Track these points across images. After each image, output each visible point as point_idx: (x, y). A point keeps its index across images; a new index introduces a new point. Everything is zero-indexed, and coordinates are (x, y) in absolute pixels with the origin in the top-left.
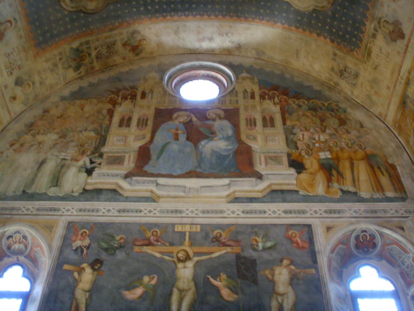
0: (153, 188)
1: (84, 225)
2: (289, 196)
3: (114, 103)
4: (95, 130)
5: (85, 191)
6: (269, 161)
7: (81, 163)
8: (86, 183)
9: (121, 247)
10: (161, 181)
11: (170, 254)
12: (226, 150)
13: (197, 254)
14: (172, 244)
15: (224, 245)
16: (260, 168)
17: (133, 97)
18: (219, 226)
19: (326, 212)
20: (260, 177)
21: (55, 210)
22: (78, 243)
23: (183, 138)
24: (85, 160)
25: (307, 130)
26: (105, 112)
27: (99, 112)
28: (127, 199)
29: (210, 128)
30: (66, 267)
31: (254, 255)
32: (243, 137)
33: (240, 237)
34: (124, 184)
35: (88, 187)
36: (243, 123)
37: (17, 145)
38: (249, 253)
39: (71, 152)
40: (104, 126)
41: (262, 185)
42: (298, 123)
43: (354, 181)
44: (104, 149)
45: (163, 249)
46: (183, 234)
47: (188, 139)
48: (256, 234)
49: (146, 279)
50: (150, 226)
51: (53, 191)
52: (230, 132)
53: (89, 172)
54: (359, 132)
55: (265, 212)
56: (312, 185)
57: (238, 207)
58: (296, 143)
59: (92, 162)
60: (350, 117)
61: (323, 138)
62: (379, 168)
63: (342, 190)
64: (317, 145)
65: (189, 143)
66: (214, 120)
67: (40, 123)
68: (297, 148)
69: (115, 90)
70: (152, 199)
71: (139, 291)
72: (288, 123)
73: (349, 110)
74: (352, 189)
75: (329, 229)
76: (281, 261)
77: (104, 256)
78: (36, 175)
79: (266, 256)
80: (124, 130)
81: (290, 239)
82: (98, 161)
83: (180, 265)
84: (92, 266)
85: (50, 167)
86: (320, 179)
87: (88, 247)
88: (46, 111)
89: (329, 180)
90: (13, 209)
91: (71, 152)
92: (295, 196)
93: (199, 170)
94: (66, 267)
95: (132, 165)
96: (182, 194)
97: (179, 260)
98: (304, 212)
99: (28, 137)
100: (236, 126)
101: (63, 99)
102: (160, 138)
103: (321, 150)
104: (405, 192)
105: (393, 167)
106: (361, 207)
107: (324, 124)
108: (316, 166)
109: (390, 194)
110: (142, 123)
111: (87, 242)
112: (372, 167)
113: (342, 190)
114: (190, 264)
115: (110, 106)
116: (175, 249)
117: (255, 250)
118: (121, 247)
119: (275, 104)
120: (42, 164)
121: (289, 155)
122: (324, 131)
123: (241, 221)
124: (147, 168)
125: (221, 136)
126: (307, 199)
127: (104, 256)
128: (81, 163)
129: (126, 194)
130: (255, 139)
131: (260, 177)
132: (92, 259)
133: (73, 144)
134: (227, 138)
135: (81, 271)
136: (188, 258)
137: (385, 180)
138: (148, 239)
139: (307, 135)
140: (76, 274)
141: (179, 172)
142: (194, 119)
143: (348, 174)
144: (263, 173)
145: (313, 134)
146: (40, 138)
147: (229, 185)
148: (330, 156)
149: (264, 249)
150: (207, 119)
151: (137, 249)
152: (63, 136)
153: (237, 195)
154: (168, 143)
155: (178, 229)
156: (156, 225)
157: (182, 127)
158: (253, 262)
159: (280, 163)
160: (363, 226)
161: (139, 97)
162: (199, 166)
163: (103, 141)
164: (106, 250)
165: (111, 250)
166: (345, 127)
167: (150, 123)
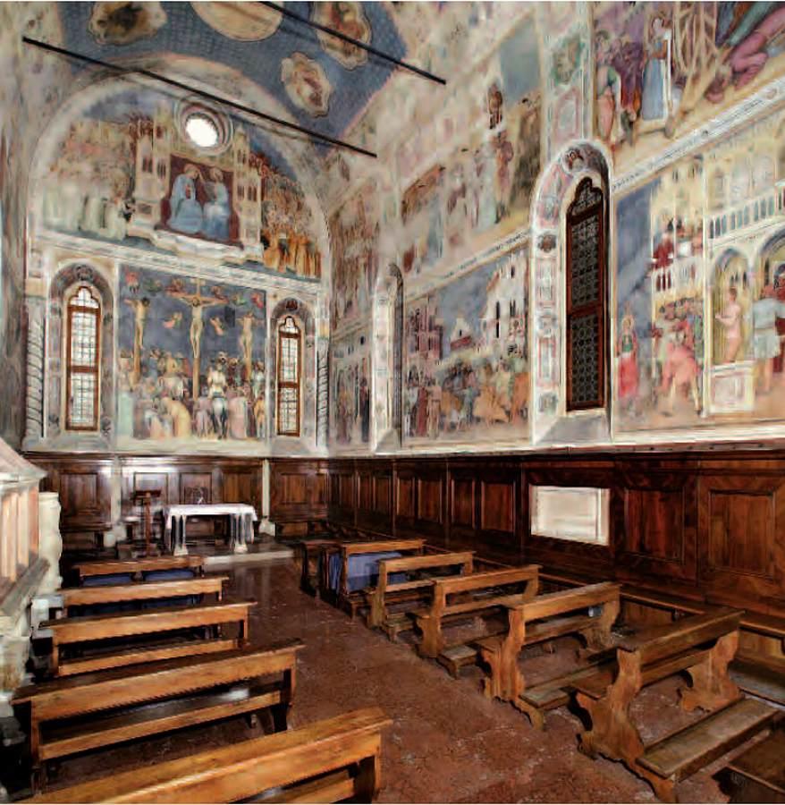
0: (172, 242)
4: (124, 169)
5: (127, 237)
9: (159, 290)
10: (180, 237)
12: (223, 217)
15: (218, 297)
16: (243, 239)
20: (242, 247)
21: (110, 252)
24: (121, 204)
27: (123, 144)
32: (234, 205)
33: (228, 295)
34: (155, 236)
35: (130, 234)
38: (233, 306)
40: (131, 166)
47: (197, 198)
49: (176, 316)
50: (176, 277)
53: (127, 217)
57: (227, 271)
58: (266, 221)
59: (128, 208)
61: (285, 219)
66: (215, 181)
69: (133, 117)
70: (173, 252)
72: (265, 199)
74: (293, 269)
76: (248, 313)
77: (149, 296)
83: (194, 308)
85: (95, 203)
86: (277, 255)
88: (73, 129)
89: (282, 258)
100: (230, 193)
103: (283, 231)
107: (289, 206)
110: (162, 171)
111: (136, 284)
116: (191, 297)
118: (159, 290)
119: (259, 174)
120: (86, 201)
121: (262, 232)
122: (286, 213)
131: (242, 247)
134: (224, 205)
135: (136, 304)
136: (198, 304)
137: (312, 265)
138: (175, 287)
140: (133, 307)
146: (76, 166)
147: (222, 251)
150: (211, 180)
152: (97, 170)
153: (230, 260)
154: (182, 200)
158: (234, 312)
159: (255, 236)
164: (150, 291)
165: (153, 292)
167: (168, 170)
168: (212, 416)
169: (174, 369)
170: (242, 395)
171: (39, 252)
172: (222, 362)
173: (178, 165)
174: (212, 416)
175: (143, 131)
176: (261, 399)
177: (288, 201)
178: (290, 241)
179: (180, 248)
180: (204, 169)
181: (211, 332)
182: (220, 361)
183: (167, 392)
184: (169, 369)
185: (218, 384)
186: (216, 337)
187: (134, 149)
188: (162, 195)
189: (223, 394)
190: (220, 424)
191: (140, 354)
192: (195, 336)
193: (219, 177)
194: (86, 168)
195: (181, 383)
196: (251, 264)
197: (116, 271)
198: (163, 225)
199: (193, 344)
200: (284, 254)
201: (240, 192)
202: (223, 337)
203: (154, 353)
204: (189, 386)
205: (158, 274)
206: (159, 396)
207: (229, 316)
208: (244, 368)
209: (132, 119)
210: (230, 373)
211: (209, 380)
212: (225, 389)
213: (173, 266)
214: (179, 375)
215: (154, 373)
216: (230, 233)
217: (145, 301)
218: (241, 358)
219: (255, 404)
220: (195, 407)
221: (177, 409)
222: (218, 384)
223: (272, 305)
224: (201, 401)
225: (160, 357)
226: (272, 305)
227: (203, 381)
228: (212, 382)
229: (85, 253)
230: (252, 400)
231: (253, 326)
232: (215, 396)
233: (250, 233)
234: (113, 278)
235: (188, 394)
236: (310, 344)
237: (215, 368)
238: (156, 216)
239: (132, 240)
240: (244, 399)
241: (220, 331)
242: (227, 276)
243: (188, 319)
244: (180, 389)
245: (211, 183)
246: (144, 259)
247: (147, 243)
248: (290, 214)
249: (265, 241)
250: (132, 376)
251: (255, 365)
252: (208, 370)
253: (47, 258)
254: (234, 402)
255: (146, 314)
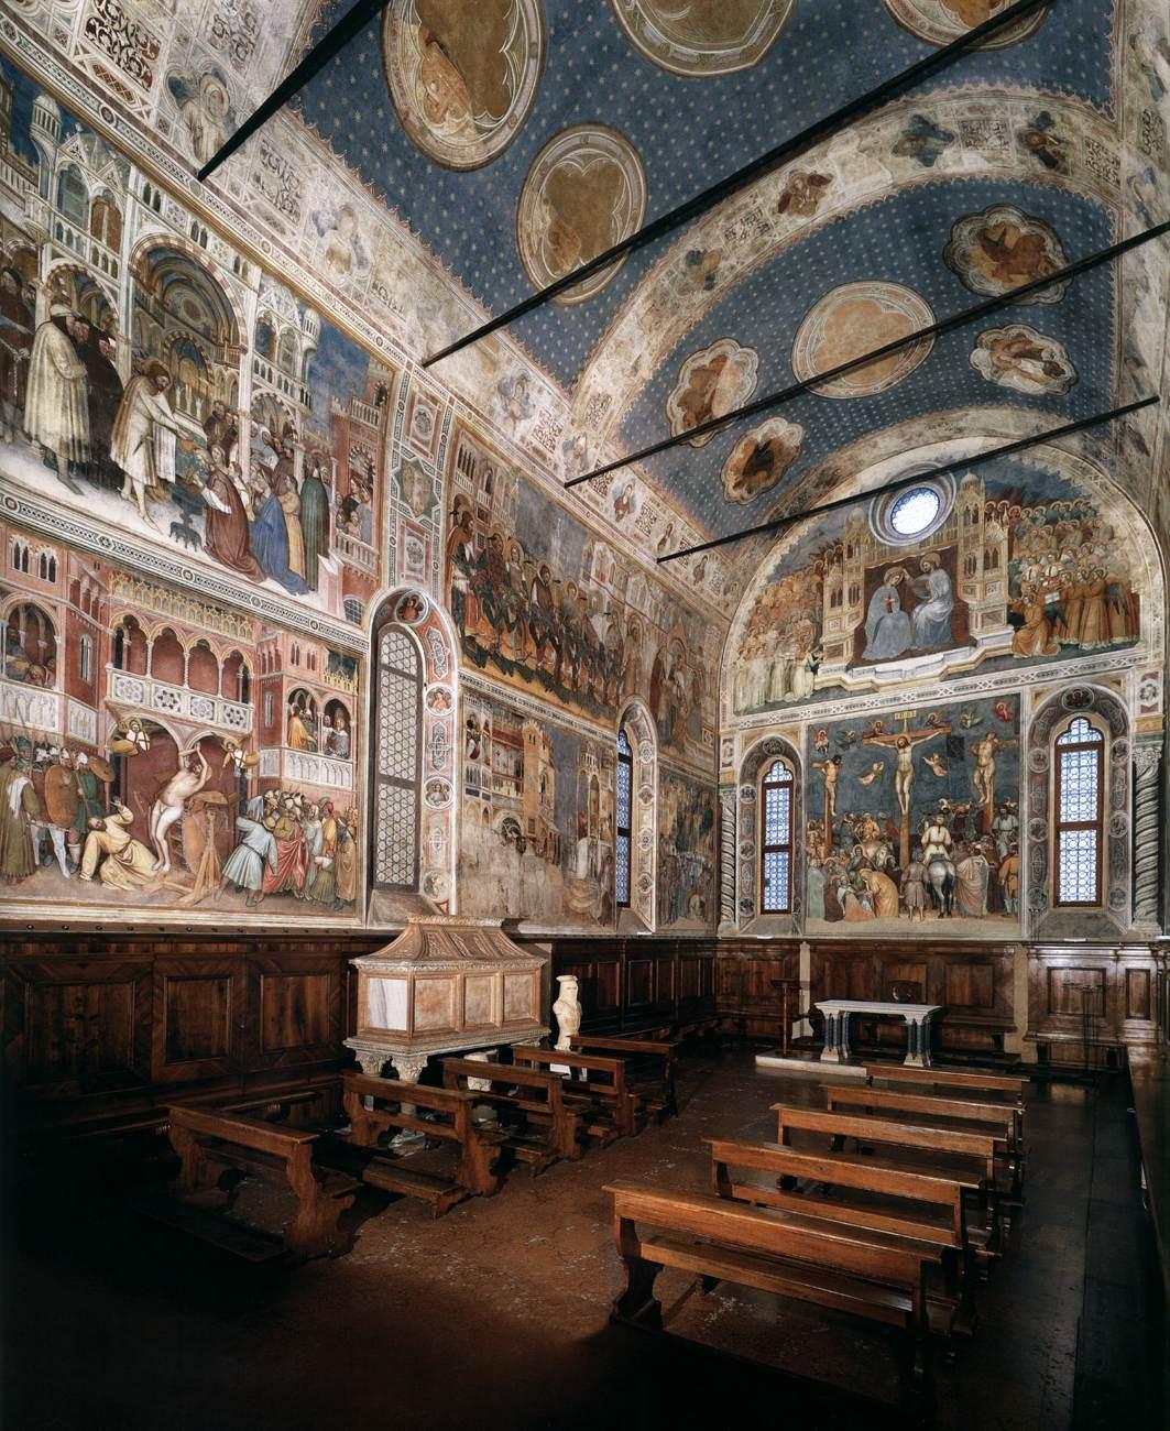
0: (871, 677)
1: (820, 726)
2: (1002, 663)
3: (821, 573)
4: (809, 617)
6: (986, 620)
7: (805, 662)
8: (815, 684)
9: (853, 741)
10: (879, 667)
11: (892, 742)
12: (942, 615)
13: (914, 739)
14: (893, 733)
15: (937, 727)
16: (976, 632)
17: (840, 556)
18: (934, 709)
19: (1038, 676)
20: (974, 644)
22: (820, 743)
23: (896, 608)
25: (1037, 562)
26: (814, 588)
28: (853, 694)
29: (924, 585)
30: (815, 765)
31: (962, 732)
32: (960, 592)
34: (846, 677)
35: (817, 688)
36: (961, 567)
37: (745, 653)
38: (959, 732)
39: (794, 650)
41: (976, 654)
42: (1027, 553)
43: (1080, 628)
44: (823, 640)
45: (886, 738)
46: (901, 721)
48: (966, 711)
49: (875, 766)
51: (789, 697)
52: (946, 587)
53: (814, 670)
54: (1106, 550)
55: (976, 686)
56: (1029, 645)
57: (949, 685)
59: (815, 659)
60: (1100, 524)
62: (1116, 604)
63: (1061, 645)
64: (1045, 584)
65: (903, 613)
66: (928, 573)
67: (757, 619)
68: (1020, 594)
69: (818, 552)
70: (873, 689)
71: (871, 777)
73: (1102, 510)
75: (1038, 695)
77: (841, 752)
78: (771, 683)
79: (973, 732)
80: (838, 610)
81: (997, 712)
82: (819, 655)
83: (901, 751)
84: (834, 761)
85: (779, 671)
86: (1040, 634)
87: (828, 746)
88: (758, 602)
89: (1050, 634)
90: (762, 721)
91: (794, 650)
92: (1008, 662)
93: (914, 648)
94: (815, 765)
95: (851, 654)
96: (900, 679)
97: (900, 747)
98: (1015, 680)
99: (751, 640)
100: (953, 576)
101: (770, 579)
102: (873, 616)
103: (1049, 590)
104: (1138, 633)
105: (1135, 598)
106: (1078, 662)
108: (1038, 617)
109: (1118, 640)
111: (826, 741)
112: (1106, 603)
113: (1061, 645)
114: (908, 749)
115: (818, 579)
116: (896, 737)
117: (964, 728)
118: (853, 741)
120: (773, 667)
121: (1009, 607)
122: (1058, 559)
123: (952, 700)
124: (864, 656)
125: (935, 596)
126: (1021, 663)
127: (841, 752)
128: (805, 662)
129: (849, 689)
130: (973, 591)
131: (974, 644)
132: (832, 756)
133: (793, 640)
134: (942, 598)
135: (826, 767)
136: (907, 744)
137: (1118, 621)
139: (1035, 568)
141: (896, 654)
142: (907, 577)
143: (1073, 625)
144: (978, 638)
145: (1043, 567)
148: (1057, 599)
149: (972, 726)
151: (866, 741)
152: (782, 632)
153: (950, 670)
155: (897, 717)
156: (878, 716)
157: (894, 592)
158: (961, 740)
160: (1076, 685)
161: (845, 555)
162: (914, 643)
163: (820, 633)
164: (841, 746)
165: (845, 746)
166: (1089, 544)
167: (861, 593)
168: (929, 887)
169: (874, 834)
170: (978, 852)
171: (731, 740)
172: (946, 813)
173: (874, 578)
174: (929, 887)
175: (831, 562)
176: (1011, 855)
177: (1060, 537)
178: (1065, 601)
179: (878, 681)
180: (913, 565)
181: (926, 776)
182: (941, 812)
183: (864, 862)
184: (867, 832)
185: (937, 844)
186: (935, 781)
187: (820, 587)
188: (851, 628)
189: (946, 856)
190: (942, 896)
191: (831, 824)
192: (903, 785)
193: (933, 563)
194: (773, 634)
195: (884, 850)
196: (991, 662)
197: (803, 736)
198: (858, 661)
199: (900, 797)
200: (1054, 625)
201: (971, 566)
202: (945, 778)
203: (849, 818)
204: (896, 852)
205: (854, 722)
206: (855, 869)
207: (955, 749)
208: (982, 814)
209: (817, 555)
210: (958, 828)
211: (924, 840)
212: (949, 849)
213: (872, 706)
214: (881, 839)
215: (849, 841)
216: (956, 631)
217: (836, 760)
218: (975, 801)
219: (1001, 865)
220: (903, 878)
221: (877, 882)
222: (937, 844)
223: (1029, 712)
224: (913, 869)
225: (856, 822)
226: (1029, 712)
227: (915, 842)
228: (929, 843)
229: (773, 726)
230: (997, 859)
231: (995, 752)
232: (936, 858)
233: (991, 617)
234: (800, 745)
235: (893, 861)
236: (1120, 751)
237: (933, 824)
238: (848, 654)
239: (821, 694)
240: (980, 859)
241: (937, 770)
242: (948, 694)
243: (892, 768)
244: (883, 857)
245: (924, 577)
246: (836, 710)
247: (839, 690)
248: (1064, 557)
249: (1016, 619)
250: (822, 849)
251: (998, 805)
252: (922, 829)
253: (737, 745)
254: (964, 865)
255: (837, 775)
